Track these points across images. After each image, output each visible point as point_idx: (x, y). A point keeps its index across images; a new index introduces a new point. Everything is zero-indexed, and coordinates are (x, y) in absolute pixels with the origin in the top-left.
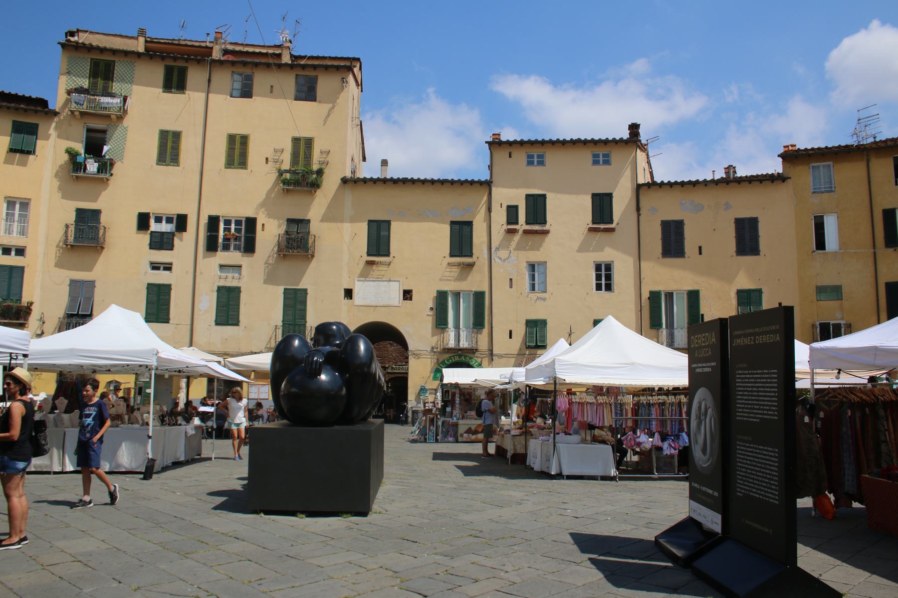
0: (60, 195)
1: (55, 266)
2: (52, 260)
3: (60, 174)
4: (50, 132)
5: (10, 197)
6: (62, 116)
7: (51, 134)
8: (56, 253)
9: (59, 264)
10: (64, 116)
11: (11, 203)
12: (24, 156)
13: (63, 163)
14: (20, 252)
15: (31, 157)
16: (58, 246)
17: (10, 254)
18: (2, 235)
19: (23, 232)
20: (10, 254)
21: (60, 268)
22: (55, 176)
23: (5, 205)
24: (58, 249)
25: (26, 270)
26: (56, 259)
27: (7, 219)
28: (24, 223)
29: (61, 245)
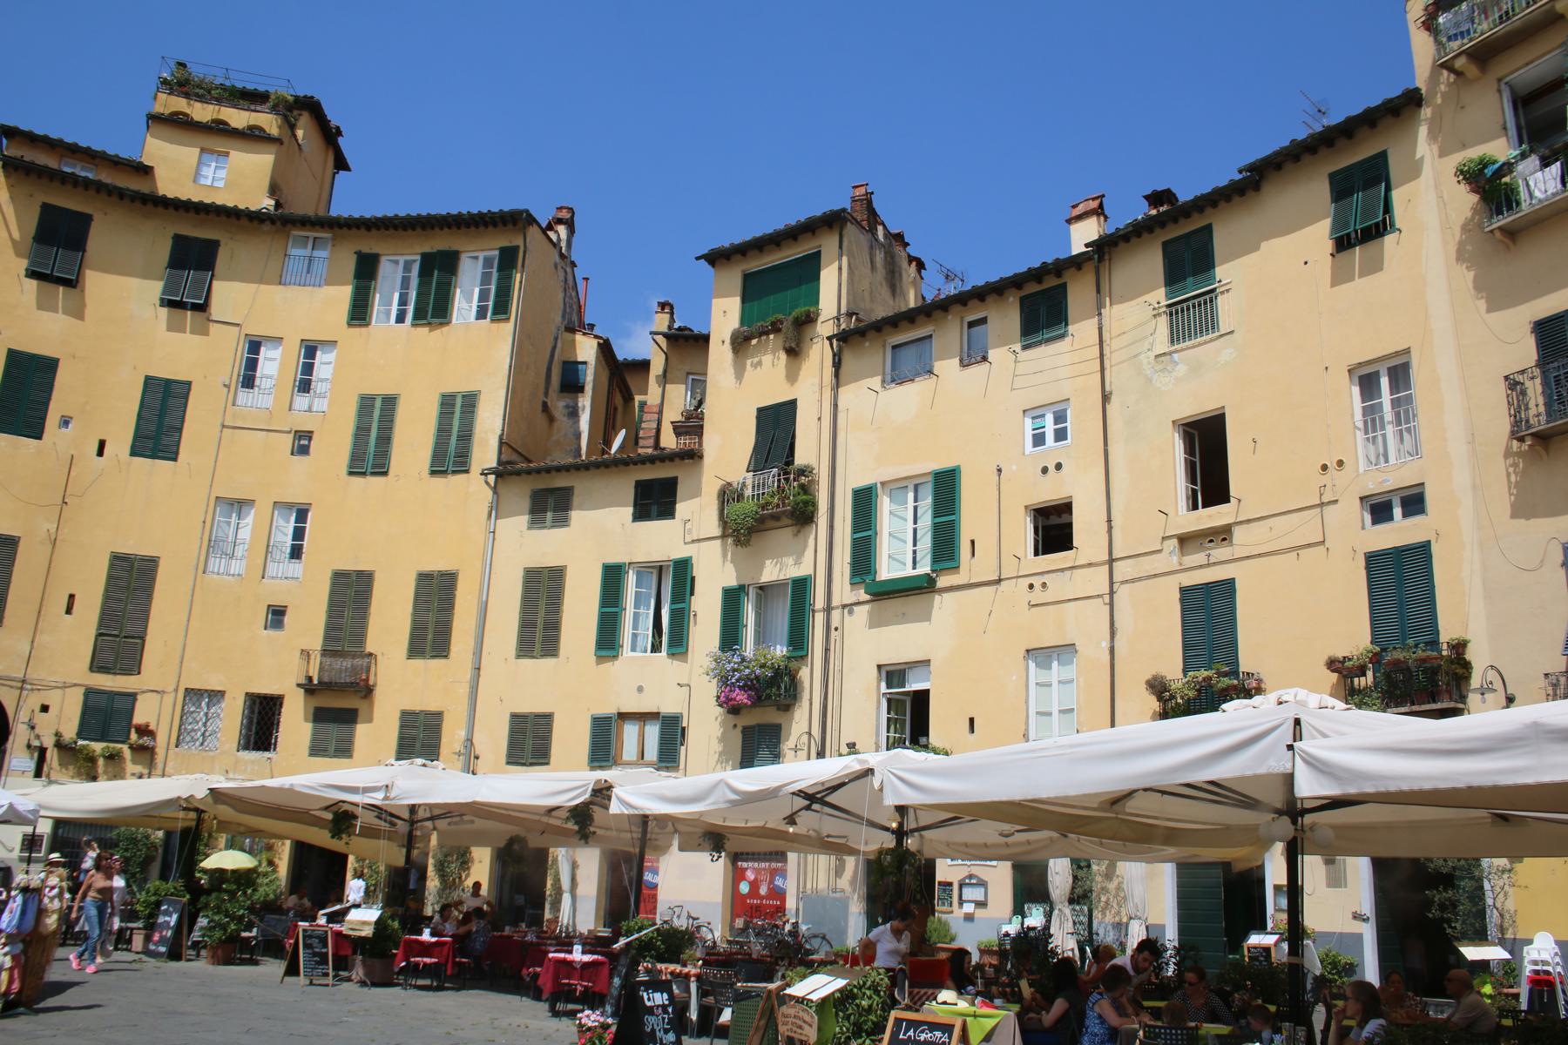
0: (1482, 304)
1: (1514, 516)
2: (1501, 499)
3: (1469, 248)
4: (1418, 156)
5: (1360, 365)
6: (1439, 95)
7: (1422, 158)
8: (1508, 475)
9: (1523, 508)
10: (1444, 95)
11: (1368, 384)
12: (1371, 246)
13: (1469, 214)
14: (1414, 502)
15: (1389, 240)
16: (1508, 453)
17: (1390, 518)
18: (1361, 470)
19: (1416, 452)
20: (1390, 518)
21: (1528, 519)
22: (1458, 259)
23: (1356, 390)
24: (1510, 461)
25: (1435, 549)
26: (1511, 494)
27: (1365, 423)
28: (1408, 422)
29: (1515, 449)
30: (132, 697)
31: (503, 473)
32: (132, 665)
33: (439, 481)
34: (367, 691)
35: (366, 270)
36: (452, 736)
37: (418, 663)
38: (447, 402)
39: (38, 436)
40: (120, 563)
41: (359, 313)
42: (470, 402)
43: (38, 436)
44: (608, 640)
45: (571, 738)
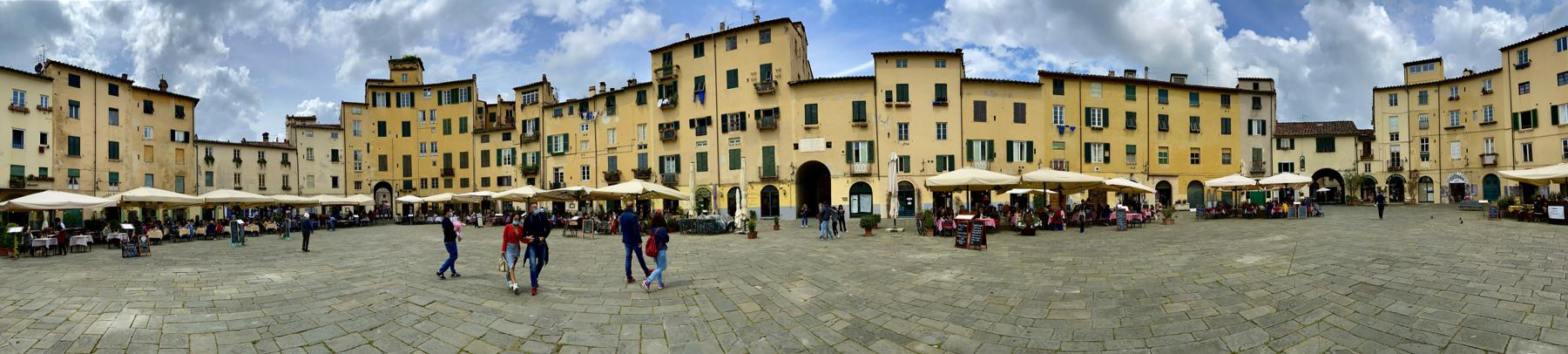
30: (411, 181)
31: (476, 132)
32: (410, 175)
33: (462, 135)
34: (453, 175)
35: (440, 94)
36: (471, 183)
37: (462, 170)
38: (461, 119)
39: (385, 136)
40: (404, 157)
41: (440, 103)
42: (466, 118)
43: (385, 136)
44: (499, 164)
45: (494, 182)
